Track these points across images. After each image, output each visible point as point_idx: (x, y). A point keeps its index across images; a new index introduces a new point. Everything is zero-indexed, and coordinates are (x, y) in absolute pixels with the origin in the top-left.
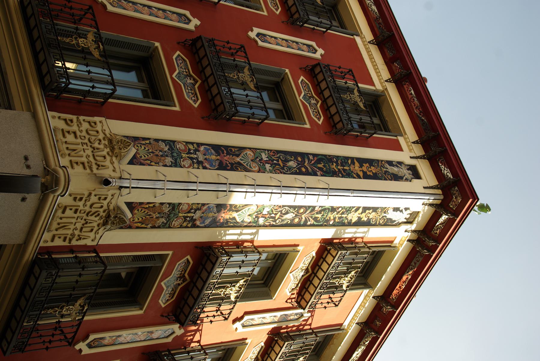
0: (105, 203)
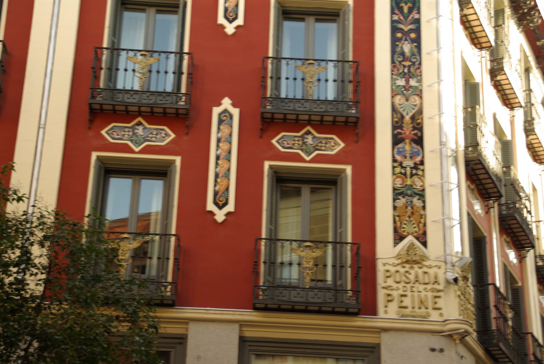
0: (393, 269)
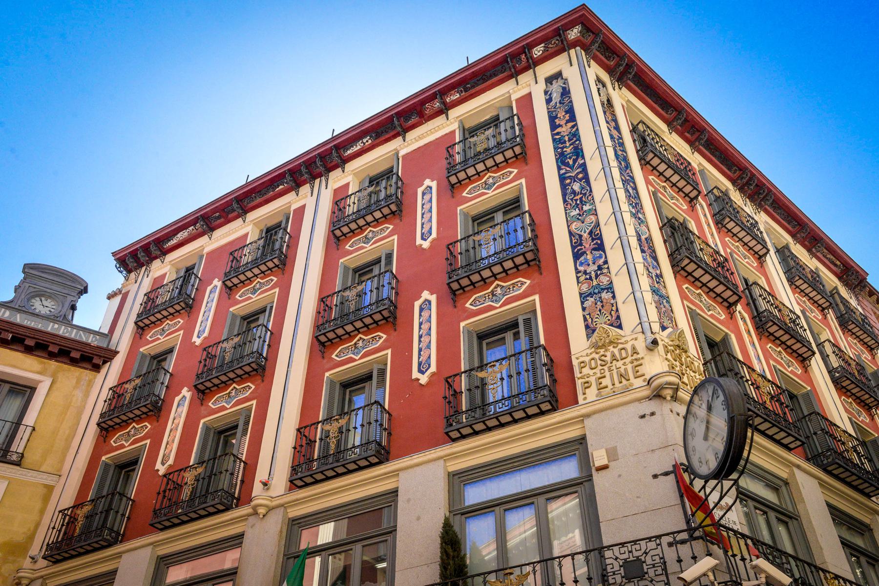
0: (587, 359)
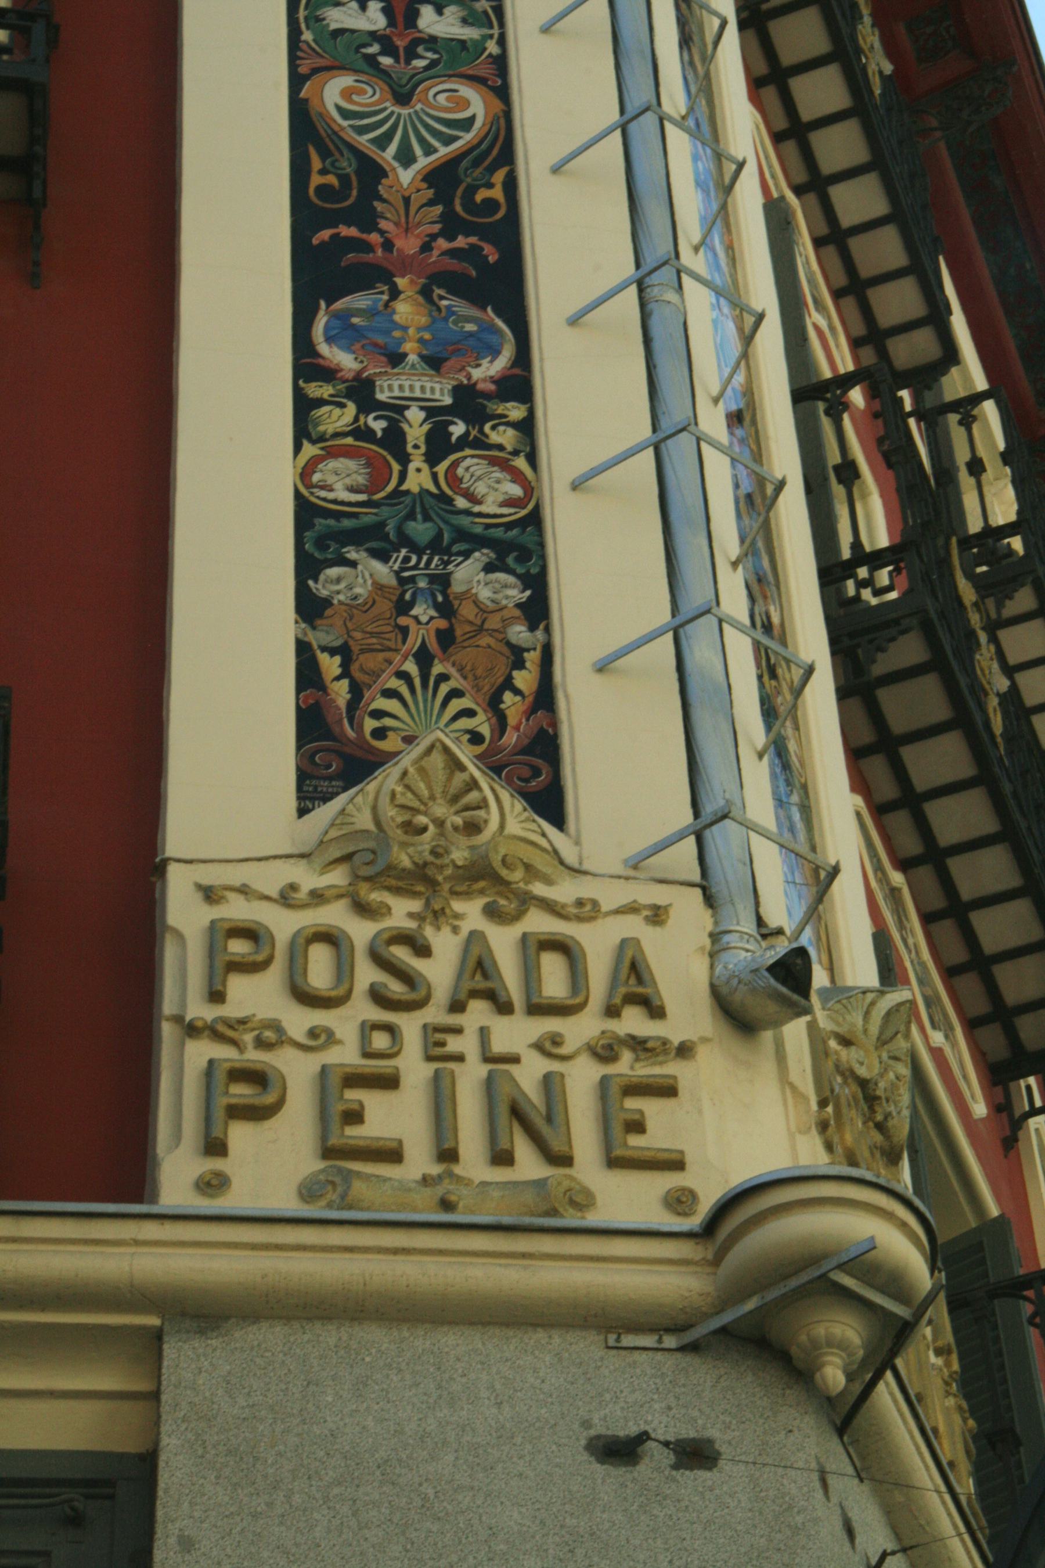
0: (284, 925)
